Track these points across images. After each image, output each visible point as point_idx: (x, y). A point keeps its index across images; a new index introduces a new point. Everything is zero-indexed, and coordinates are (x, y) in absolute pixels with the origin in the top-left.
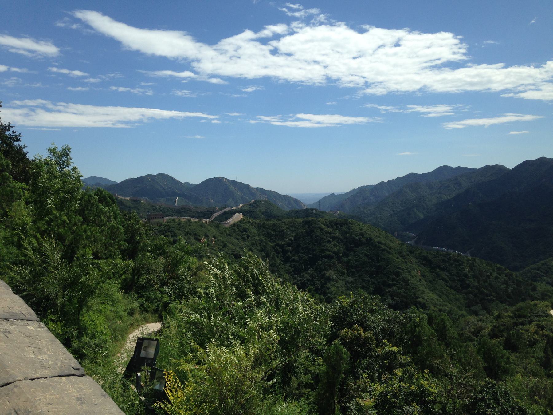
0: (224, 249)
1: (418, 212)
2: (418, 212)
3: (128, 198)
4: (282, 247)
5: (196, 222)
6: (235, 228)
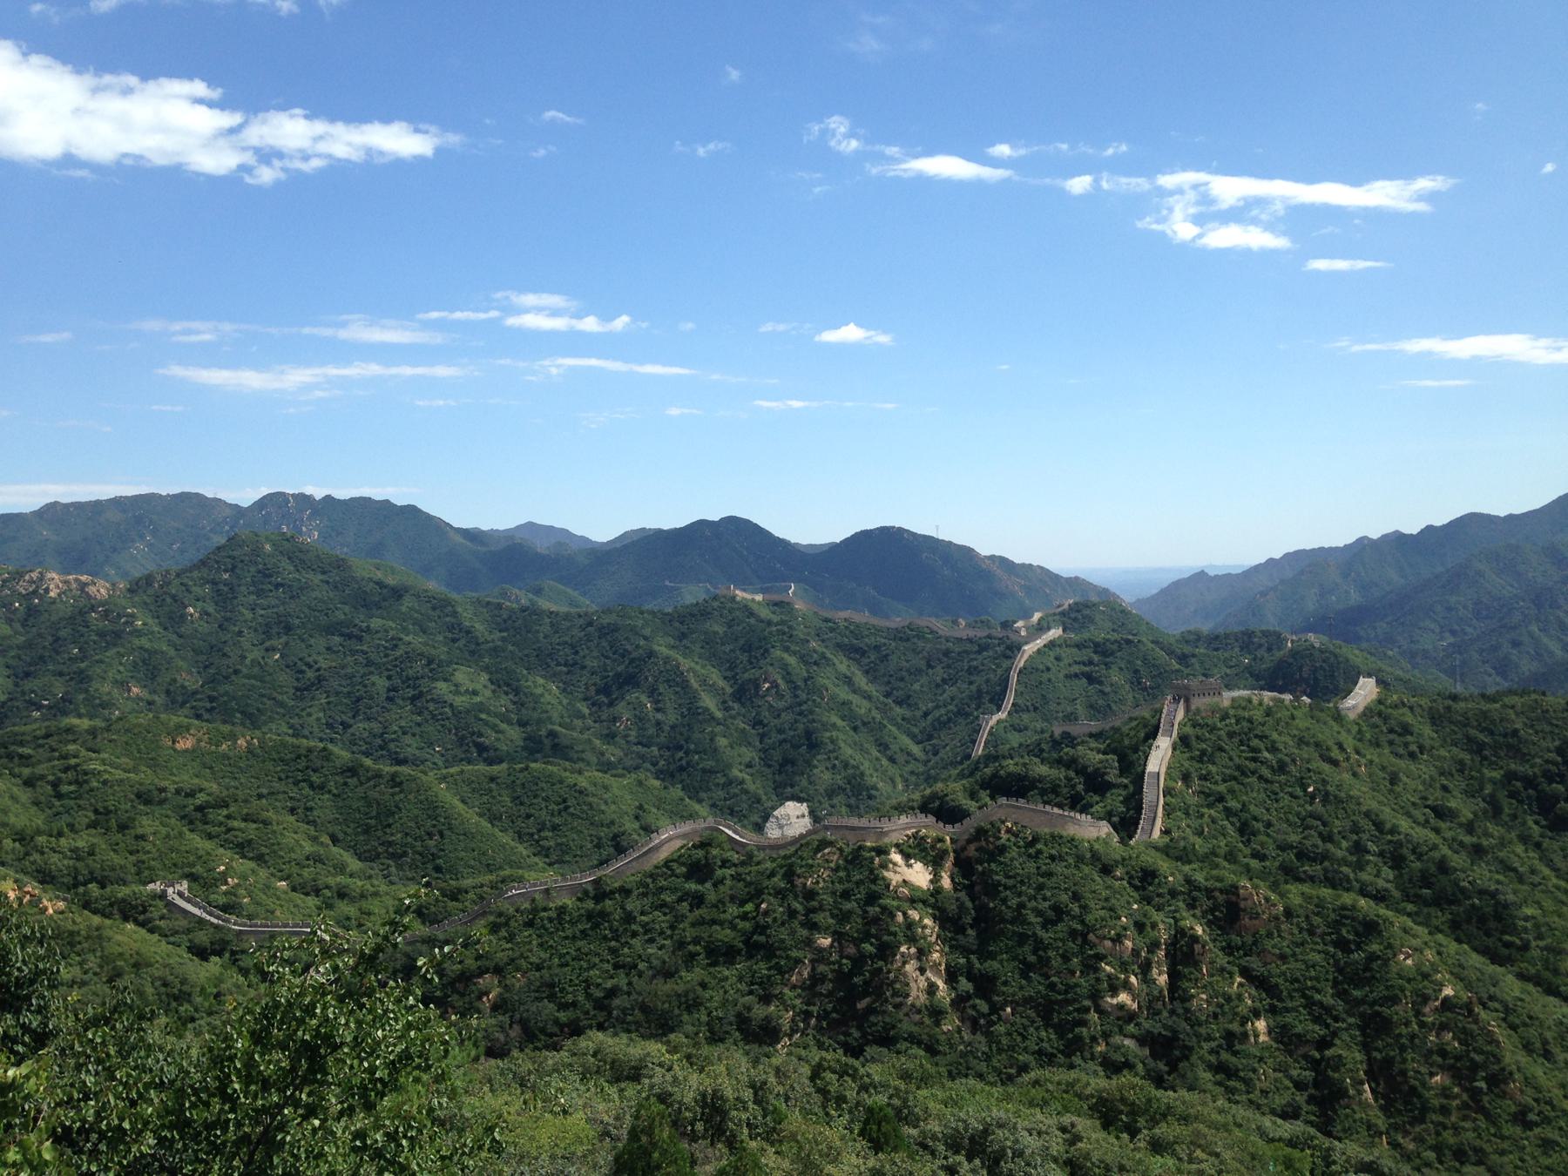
1: (1545, 640)
2: (1545, 640)
4: (1529, 782)
6: (1376, 720)
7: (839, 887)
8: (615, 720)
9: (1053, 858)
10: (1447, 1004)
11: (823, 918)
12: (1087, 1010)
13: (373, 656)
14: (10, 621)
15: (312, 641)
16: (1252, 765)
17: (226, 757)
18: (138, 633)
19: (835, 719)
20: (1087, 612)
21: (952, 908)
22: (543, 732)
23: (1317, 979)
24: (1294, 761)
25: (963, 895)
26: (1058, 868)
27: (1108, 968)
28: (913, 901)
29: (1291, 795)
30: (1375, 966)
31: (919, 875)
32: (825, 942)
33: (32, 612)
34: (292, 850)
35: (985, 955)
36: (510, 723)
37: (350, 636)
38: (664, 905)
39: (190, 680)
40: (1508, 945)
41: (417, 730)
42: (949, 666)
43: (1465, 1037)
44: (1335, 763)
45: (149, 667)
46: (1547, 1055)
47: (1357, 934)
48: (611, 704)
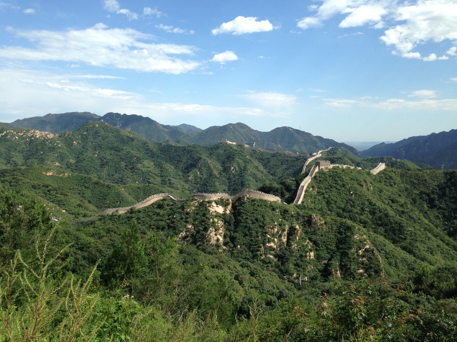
0: (381, 194)
3: (234, 143)
4: (428, 195)
5: (353, 170)
7: (196, 212)
8: (188, 176)
9: (258, 206)
10: (366, 250)
11: (189, 220)
12: (261, 247)
13: (122, 156)
14: (25, 144)
15: (106, 152)
16: (334, 185)
17: (61, 178)
18: (59, 148)
19: (252, 179)
20: (335, 151)
21: (228, 219)
22: (167, 179)
23: (331, 242)
24: (348, 184)
25: (232, 216)
26: (259, 208)
27: (268, 236)
28: (216, 216)
29: (345, 194)
30: (347, 239)
31: (220, 210)
32: (190, 226)
33: (31, 141)
34: (73, 203)
35: (235, 231)
36: (158, 176)
37: (116, 151)
38: (149, 216)
39: (72, 161)
40: (400, 238)
41: (131, 177)
42: (287, 165)
43: (370, 259)
44: (362, 186)
45: (61, 158)
46: (396, 266)
47: (345, 230)
48: (188, 172)
